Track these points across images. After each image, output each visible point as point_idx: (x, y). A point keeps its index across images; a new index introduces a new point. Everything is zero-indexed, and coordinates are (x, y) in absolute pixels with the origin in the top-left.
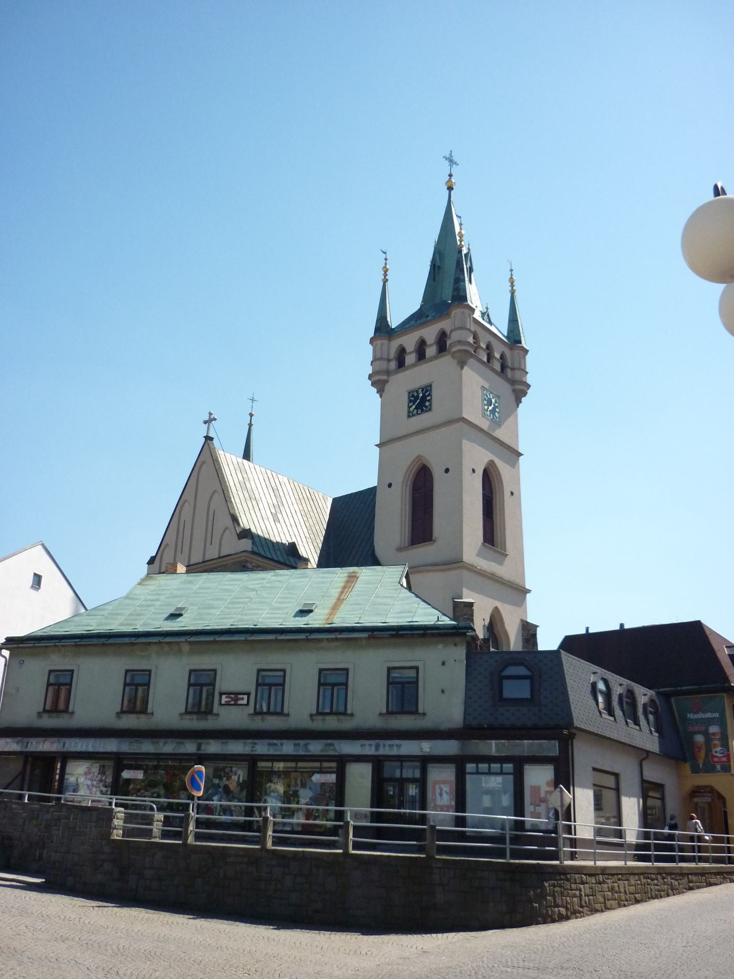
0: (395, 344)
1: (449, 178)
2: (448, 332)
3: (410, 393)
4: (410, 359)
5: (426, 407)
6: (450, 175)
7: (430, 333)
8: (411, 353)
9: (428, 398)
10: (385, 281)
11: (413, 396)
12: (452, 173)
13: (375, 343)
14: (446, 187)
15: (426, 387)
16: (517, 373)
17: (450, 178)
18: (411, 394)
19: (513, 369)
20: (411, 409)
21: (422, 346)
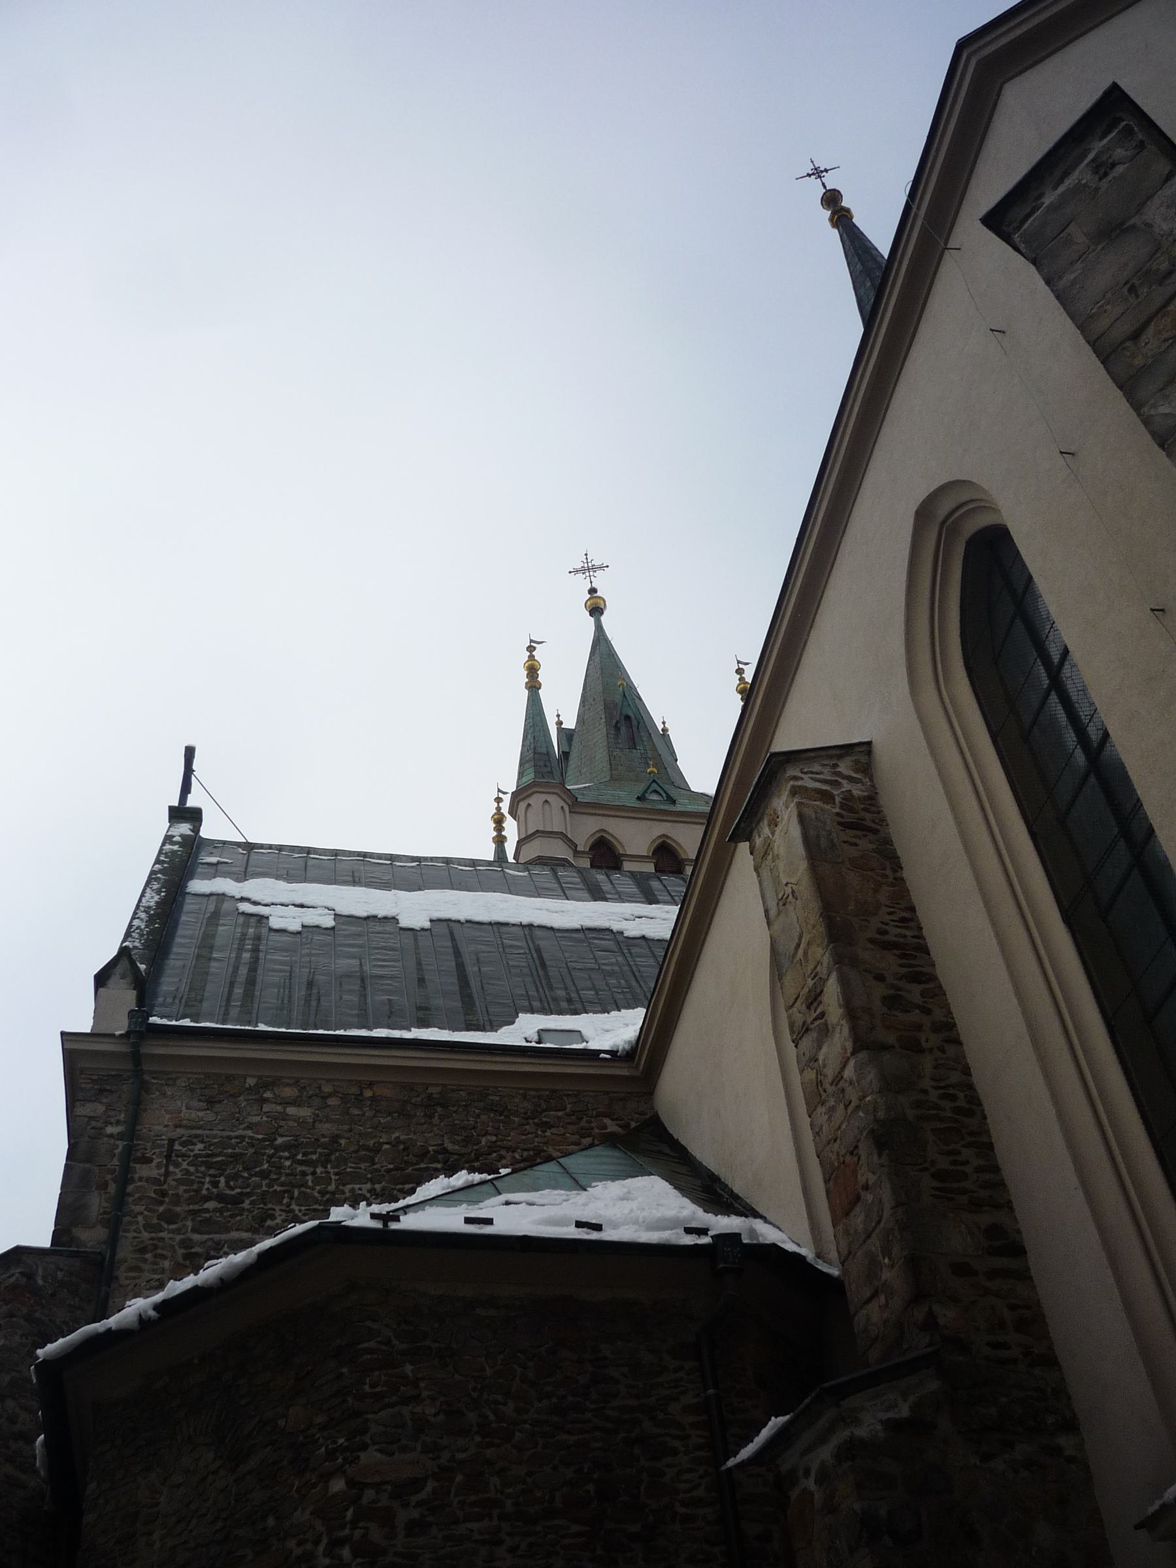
10: (533, 686)
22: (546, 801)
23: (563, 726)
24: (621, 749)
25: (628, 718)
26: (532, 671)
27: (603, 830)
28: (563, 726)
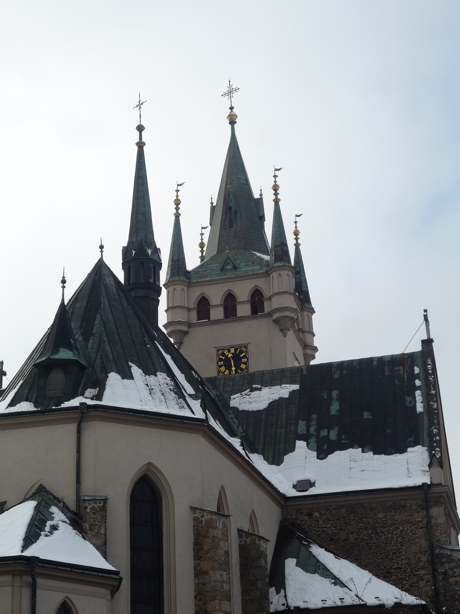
0: (196, 293)
1: (230, 111)
2: (266, 294)
3: (219, 351)
5: (242, 370)
6: (232, 108)
9: (244, 360)
10: (177, 216)
11: (223, 354)
12: (233, 106)
13: (171, 288)
14: (229, 122)
15: (241, 347)
16: (307, 335)
17: (232, 111)
18: (220, 352)
19: (303, 332)
20: (223, 369)
22: (175, 289)
24: (226, 229)
25: (230, 208)
26: (177, 203)
27: (203, 293)
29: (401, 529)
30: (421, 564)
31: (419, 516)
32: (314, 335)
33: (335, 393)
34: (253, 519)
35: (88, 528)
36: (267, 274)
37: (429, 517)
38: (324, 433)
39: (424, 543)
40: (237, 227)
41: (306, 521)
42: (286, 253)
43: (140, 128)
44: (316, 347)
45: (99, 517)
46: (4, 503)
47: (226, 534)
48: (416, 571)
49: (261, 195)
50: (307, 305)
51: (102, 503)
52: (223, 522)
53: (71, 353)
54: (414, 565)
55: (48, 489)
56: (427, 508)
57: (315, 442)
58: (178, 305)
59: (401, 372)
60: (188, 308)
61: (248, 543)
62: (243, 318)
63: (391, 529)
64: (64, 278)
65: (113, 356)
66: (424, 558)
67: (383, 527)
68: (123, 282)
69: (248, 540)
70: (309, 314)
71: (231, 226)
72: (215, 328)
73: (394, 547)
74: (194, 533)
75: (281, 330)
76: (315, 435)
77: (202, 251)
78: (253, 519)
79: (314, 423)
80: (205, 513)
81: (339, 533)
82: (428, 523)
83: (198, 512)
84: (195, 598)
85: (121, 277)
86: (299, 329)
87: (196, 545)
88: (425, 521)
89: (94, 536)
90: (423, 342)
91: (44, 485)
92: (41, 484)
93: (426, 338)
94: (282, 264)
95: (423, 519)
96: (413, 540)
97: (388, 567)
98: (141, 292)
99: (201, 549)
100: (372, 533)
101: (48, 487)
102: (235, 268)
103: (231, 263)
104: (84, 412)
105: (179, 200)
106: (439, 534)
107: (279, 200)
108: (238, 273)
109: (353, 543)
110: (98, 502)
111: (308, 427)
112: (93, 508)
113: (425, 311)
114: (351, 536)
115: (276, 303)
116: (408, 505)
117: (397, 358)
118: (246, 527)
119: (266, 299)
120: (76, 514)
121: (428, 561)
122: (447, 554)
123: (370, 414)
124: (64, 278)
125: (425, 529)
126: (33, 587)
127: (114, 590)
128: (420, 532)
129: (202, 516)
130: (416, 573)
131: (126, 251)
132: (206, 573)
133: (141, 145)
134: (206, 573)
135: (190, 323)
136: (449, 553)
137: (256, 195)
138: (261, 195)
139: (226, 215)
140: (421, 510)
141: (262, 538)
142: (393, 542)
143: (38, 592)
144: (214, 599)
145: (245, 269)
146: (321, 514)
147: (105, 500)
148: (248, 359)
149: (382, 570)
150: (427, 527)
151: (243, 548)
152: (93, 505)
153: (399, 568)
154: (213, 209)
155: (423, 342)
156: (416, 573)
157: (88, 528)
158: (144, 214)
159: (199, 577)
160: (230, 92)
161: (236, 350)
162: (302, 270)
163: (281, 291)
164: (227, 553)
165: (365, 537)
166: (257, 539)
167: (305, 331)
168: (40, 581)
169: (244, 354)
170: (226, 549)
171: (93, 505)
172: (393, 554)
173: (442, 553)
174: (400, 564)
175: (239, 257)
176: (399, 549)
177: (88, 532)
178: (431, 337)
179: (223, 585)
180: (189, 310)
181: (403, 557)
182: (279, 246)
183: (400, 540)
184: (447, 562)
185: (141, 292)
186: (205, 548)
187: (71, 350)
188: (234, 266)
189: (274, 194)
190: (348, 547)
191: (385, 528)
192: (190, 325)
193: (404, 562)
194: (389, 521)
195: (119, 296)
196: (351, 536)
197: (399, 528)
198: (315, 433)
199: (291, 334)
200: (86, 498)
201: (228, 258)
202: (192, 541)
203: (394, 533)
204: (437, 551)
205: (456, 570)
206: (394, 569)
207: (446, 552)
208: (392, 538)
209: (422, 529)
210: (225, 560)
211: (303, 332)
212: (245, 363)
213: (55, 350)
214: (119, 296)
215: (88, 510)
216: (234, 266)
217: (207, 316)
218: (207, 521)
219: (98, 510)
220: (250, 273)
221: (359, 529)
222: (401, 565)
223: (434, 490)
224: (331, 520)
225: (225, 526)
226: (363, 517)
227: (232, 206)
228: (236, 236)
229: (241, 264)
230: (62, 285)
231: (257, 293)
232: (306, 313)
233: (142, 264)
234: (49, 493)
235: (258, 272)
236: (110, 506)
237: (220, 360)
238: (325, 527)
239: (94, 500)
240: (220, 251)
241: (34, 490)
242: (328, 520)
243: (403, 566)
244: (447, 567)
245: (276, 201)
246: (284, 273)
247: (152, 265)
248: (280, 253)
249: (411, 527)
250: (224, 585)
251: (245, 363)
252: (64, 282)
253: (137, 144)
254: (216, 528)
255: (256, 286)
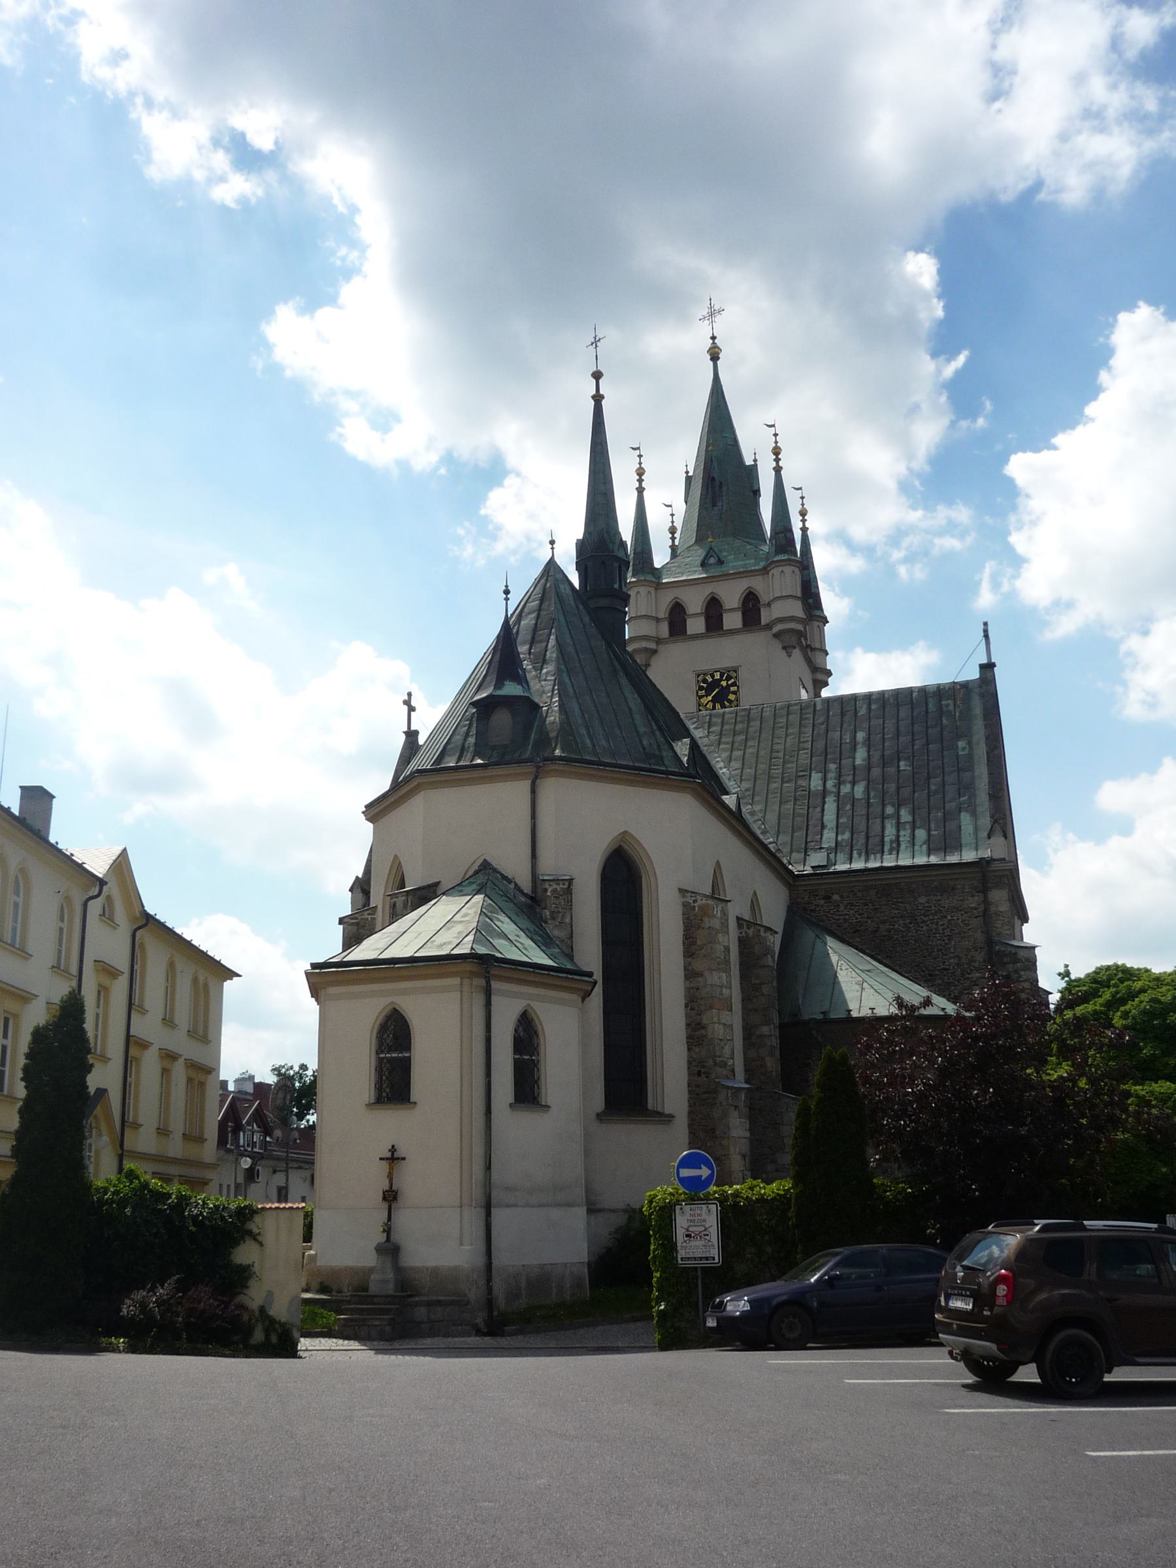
2: (764, 598)
3: (698, 676)
4: (696, 625)
5: (730, 701)
7: (731, 595)
8: (696, 615)
11: (705, 681)
12: (715, 335)
14: (709, 357)
15: (729, 671)
16: (817, 653)
18: (700, 678)
20: (704, 701)
21: (713, 611)
23: (690, 474)
25: (713, 479)
28: (690, 474)
29: (949, 917)
30: (976, 964)
31: (973, 902)
32: (827, 654)
33: (861, 736)
34: (754, 905)
35: (548, 917)
36: (765, 571)
37: (986, 903)
38: (846, 789)
39: (979, 936)
40: (722, 505)
41: (822, 906)
42: (792, 541)
43: (597, 376)
44: (830, 670)
45: (563, 903)
46: (437, 884)
47: (725, 925)
48: (969, 974)
49: (755, 460)
50: (817, 613)
51: (567, 883)
52: (722, 908)
53: (520, 687)
54: (965, 966)
55: (495, 866)
56: (984, 890)
57: (834, 801)
58: (643, 614)
59: (951, 708)
60: (657, 618)
61: (751, 935)
62: (732, 632)
63: (936, 917)
64: (507, 586)
65: (574, 690)
66: (980, 957)
67: (925, 915)
68: (578, 588)
69: (751, 932)
70: (821, 624)
71: (714, 505)
72: (695, 644)
73: (939, 942)
74: (684, 923)
75: (784, 648)
76: (833, 792)
77: (673, 539)
78: (754, 905)
79: (831, 775)
80: (698, 897)
81: (866, 922)
82: (985, 910)
83: (689, 895)
84: (686, 1006)
85: (576, 584)
86: (808, 646)
87: (686, 939)
88: (982, 908)
89: (556, 926)
90: (982, 667)
91: (489, 860)
92: (485, 860)
93: (985, 661)
94: (786, 557)
95: (979, 905)
96: (965, 932)
97: (931, 968)
98: (604, 602)
99: (694, 943)
100: (910, 923)
101: (494, 864)
102: (720, 562)
103: (714, 554)
104: (540, 767)
105: (643, 469)
106: (1000, 926)
107: (781, 468)
108: (725, 569)
109: (885, 936)
110: (561, 883)
111: (825, 781)
112: (554, 891)
113: (986, 624)
114: (881, 926)
115: (779, 610)
116: (959, 886)
117: (945, 688)
118: (747, 916)
119: (764, 605)
120: (532, 898)
121: (984, 961)
122: (1010, 952)
123: (908, 764)
124: (507, 586)
125: (981, 919)
126: (488, 993)
127: (586, 995)
128: (974, 922)
129: (695, 901)
130: (968, 976)
131: (581, 546)
132: (700, 974)
133: (598, 398)
134: (700, 974)
135: (659, 639)
136: (1013, 951)
137: (749, 461)
138: (755, 460)
139: (707, 489)
140: (977, 894)
141: (768, 929)
142: (938, 935)
143: (494, 999)
144: (711, 1008)
145: (734, 564)
146: (842, 897)
147: (571, 881)
148: (738, 687)
149: (924, 971)
150: (984, 915)
151: (743, 942)
152: (555, 886)
153: (944, 969)
154: (689, 480)
155: (982, 667)
156: (968, 976)
157: (548, 917)
158: (605, 494)
159: (692, 979)
160: (712, 314)
161: (722, 675)
162: (811, 564)
163: (784, 594)
164: (727, 949)
165: (901, 928)
166: (762, 930)
167: (815, 648)
168: (495, 985)
169: (733, 680)
170: (727, 944)
171: (555, 886)
172: (938, 951)
173: (1004, 951)
174: (947, 963)
175: (726, 547)
176: (946, 944)
177: (549, 922)
178: (993, 661)
179: (722, 991)
180: (658, 620)
181: (952, 955)
182: (781, 533)
183: (948, 932)
184: (1010, 963)
185: (604, 602)
186: (699, 943)
187: (520, 683)
188: (719, 559)
189: (774, 460)
190: (878, 941)
191: (928, 916)
192: (659, 641)
193: (952, 961)
194: (933, 908)
195: (578, 608)
196: (881, 926)
197: (946, 917)
198: (834, 790)
199: (797, 653)
200: (545, 878)
201: (711, 549)
202: (682, 933)
203: (940, 923)
204: (997, 948)
205: (1022, 973)
206: (939, 970)
207: (1009, 949)
208: (936, 929)
209: (978, 919)
210: (725, 957)
211: (813, 649)
212: (734, 693)
213: (499, 685)
214: (578, 608)
215: (549, 894)
216: (719, 559)
217: (683, 631)
218: (700, 907)
219: (562, 893)
220: (741, 570)
221: (893, 917)
222: (950, 965)
223: (995, 866)
224: (856, 906)
225: (725, 914)
226: (898, 902)
227: (715, 476)
228: (721, 518)
229: (729, 557)
230: (505, 596)
231: (751, 597)
232: (816, 624)
233: (603, 563)
234: (495, 870)
235: (753, 568)
236: (576, 886)
237: (701, 688)
238: (847, 915)
239: (556, 881)
240: (699, 540)
241: (476, 867)
242: (852, 905)
243: (951, 967)
244: (1011, 970)
245: (778, 470)
246: (788, 569)
247: (616, 565)
248: (783, 542)
249: (962, 915)
250: (724, 989)
251: (734, 693)
252: (507, 592)
253: (593, 397)
254: (714, 916)
255: (749, 587)
